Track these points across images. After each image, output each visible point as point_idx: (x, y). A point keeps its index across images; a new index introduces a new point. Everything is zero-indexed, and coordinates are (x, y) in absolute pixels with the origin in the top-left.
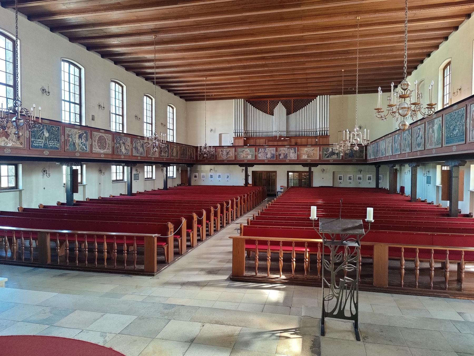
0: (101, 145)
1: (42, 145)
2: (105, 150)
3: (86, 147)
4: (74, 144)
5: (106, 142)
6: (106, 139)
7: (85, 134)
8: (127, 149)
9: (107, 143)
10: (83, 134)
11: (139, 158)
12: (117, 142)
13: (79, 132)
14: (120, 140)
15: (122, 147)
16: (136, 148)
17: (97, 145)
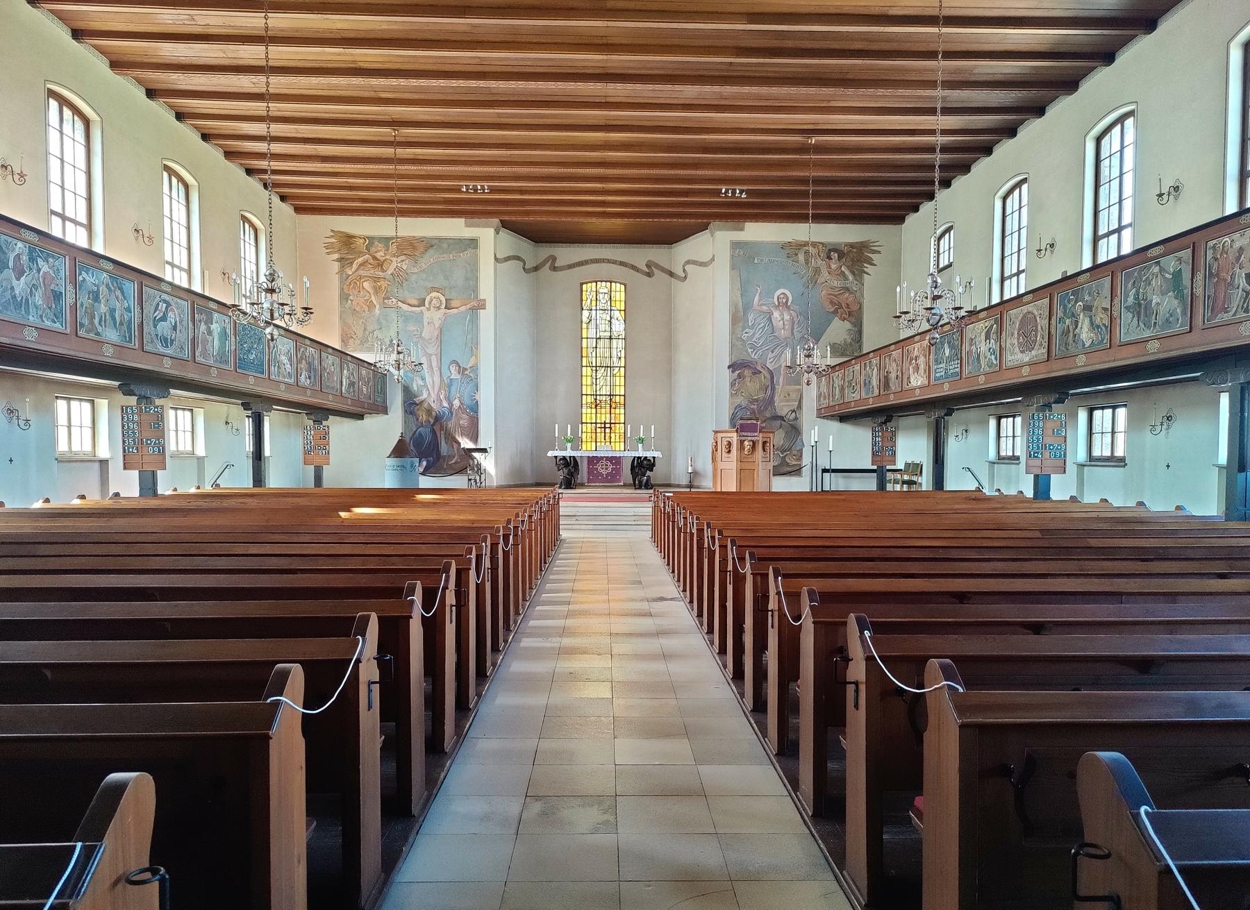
0: (1024, 340)
1: (943, 374)
2: (1034, 353)
3: (996, 359)
4: (979, 355)
5: (1037, 327)
6: (1038, 318)
7: (995, 325)
8: (1098, 327)
9: (1039, 328)
10: (992, 326)
11: (1153, 346)
12: (1065, 313)
13: (987, 324)
14: (1076, 302)
15: (1080, 324)
16: (1141, 309)
17: (1016, 343)
